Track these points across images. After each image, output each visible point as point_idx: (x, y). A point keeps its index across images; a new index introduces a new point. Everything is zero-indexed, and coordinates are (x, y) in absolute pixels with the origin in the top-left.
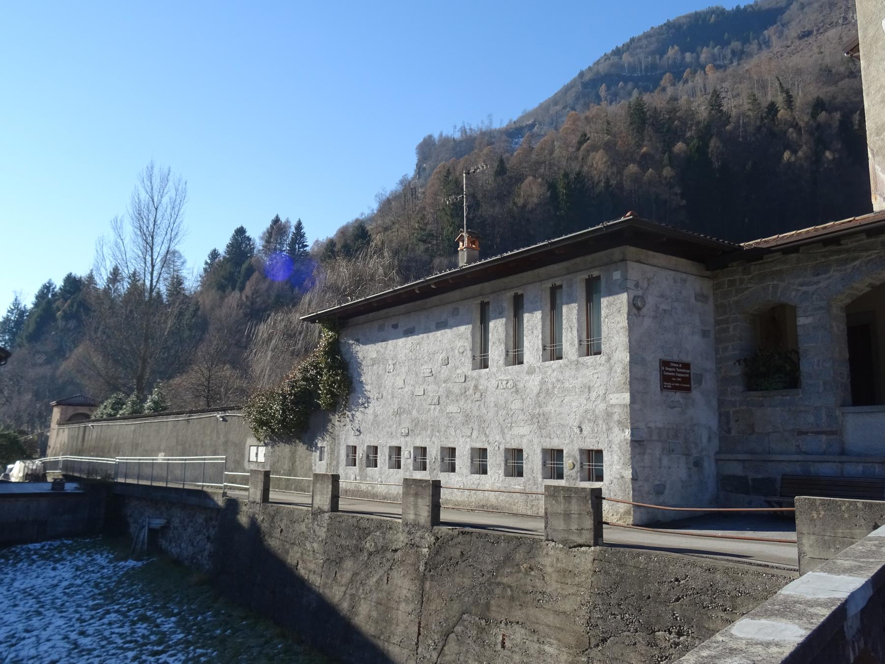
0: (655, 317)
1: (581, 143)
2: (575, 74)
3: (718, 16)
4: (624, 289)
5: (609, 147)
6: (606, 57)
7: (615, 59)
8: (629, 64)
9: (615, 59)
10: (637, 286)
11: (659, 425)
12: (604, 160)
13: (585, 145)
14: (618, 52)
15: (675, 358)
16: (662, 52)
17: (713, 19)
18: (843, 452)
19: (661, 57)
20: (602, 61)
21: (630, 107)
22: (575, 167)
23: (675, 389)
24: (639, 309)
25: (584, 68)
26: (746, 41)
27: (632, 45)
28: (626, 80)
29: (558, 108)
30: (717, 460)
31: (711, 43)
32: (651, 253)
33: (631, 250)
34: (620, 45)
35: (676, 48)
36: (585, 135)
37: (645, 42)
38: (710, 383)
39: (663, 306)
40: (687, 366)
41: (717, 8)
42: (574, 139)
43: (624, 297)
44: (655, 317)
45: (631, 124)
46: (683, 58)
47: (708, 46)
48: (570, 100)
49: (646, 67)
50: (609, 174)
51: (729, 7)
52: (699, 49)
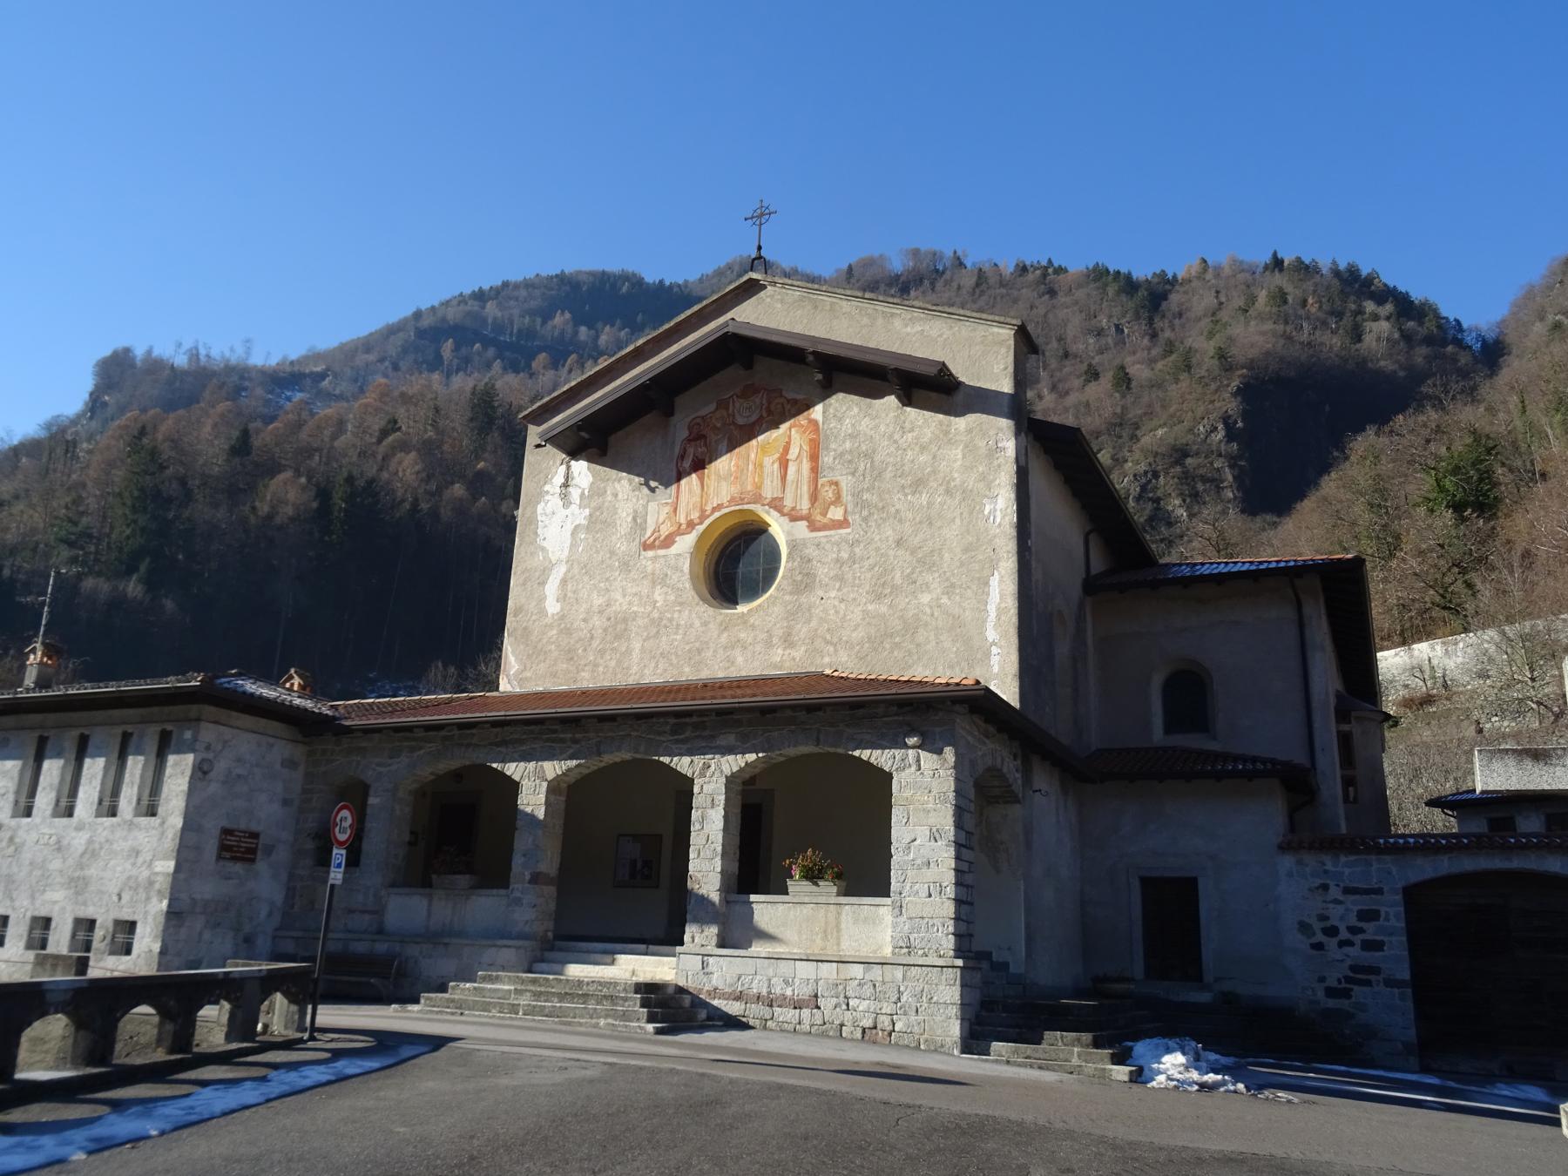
0: (224, 783)
2: (408, 312)
3: (633, 285)
4: (193, 750)
10: (208, 748)
11: (207, 896)
15: (243, 826)
17: (624, 289)
18: (381, 931)
23: (233, 859)
24: (205, 773)
30: (274, 938)
32: (234, 714)
33: (209, 710)
36: (396, 422)
38: (282, 855)
39: (239, 771)
40: (255, 835)
43: (190, 758)
44: (224, 783)
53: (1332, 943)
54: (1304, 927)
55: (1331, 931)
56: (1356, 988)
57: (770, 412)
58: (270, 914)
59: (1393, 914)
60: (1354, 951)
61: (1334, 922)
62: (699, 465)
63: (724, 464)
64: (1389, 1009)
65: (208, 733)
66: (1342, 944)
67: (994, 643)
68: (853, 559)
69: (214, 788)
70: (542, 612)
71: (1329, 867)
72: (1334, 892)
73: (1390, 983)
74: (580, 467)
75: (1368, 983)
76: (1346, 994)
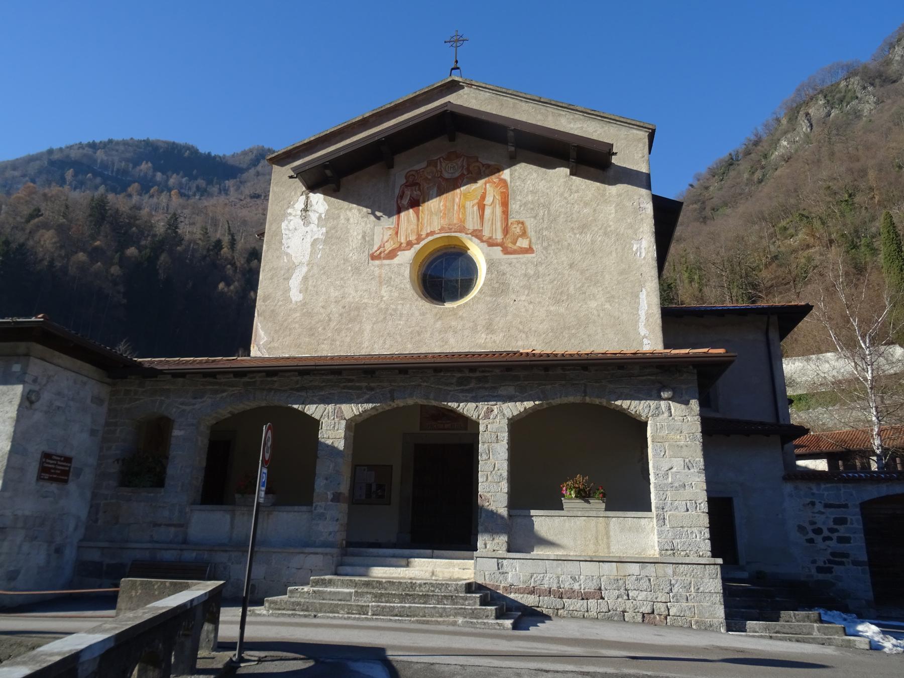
0: (46, 412)
1: (32, 217)
4: (20, 380)
5: (61, 230)
6: (81, 146)
7: (89, 151)
8: (102, 161)
9: (89, 151)
10: (35, 381)
11: (27, 513)
12: (54, 240)
13: (36, 220)
14: (93, 146)
15: (59, 452)
16: (136, 163)
18: (185, 542)
19: (134, 167)
20: (76, 147)
21: (92, 200)
22: (20, 237)
23: (51, 480)
24: (32, 403)
25: (56, 146)
26: (210, 182)
27: (108, 145)
28: (96, 174)
29: (16, 173)
30: (79, 547)
31: (181, 173)
32: (57, 353)
33: (38, 348)
34: (97, 141)
35: (150, 164)
37: (122, 148)
38: (88, 476)
39: (58, 403)
40: (68, 460)
41: (193, 147)
42: (26, 211)
43: (19, 389)
44: (46, 412)
45: (90, 215)
46: (154, 176)
47: (178, 174)
48: (32, 169)
49: (118, 170)
50: (56, 255)
51: (203, 149)
52: (169, 173)
53: (818, 539)
54: (801, 529)
55: (818, 531)
56: (835, 566)
57: (469, 171)
58: (76, 528)
59: (855, 520)
60: (833, 544)
61: (819, 525)
62: (415, 203)
63: (434, 205)
64: (856, 579)
65: (36, 367)
66: (826, 539)
67: (645, 337)
68: (537, 275)
69: (38, 416)
70: (288, 300)
71: (815, 491)
72: (819, 507)
73: (856, 563)
74: (318, 200)
75: (842, 563)
76: (829, 570)
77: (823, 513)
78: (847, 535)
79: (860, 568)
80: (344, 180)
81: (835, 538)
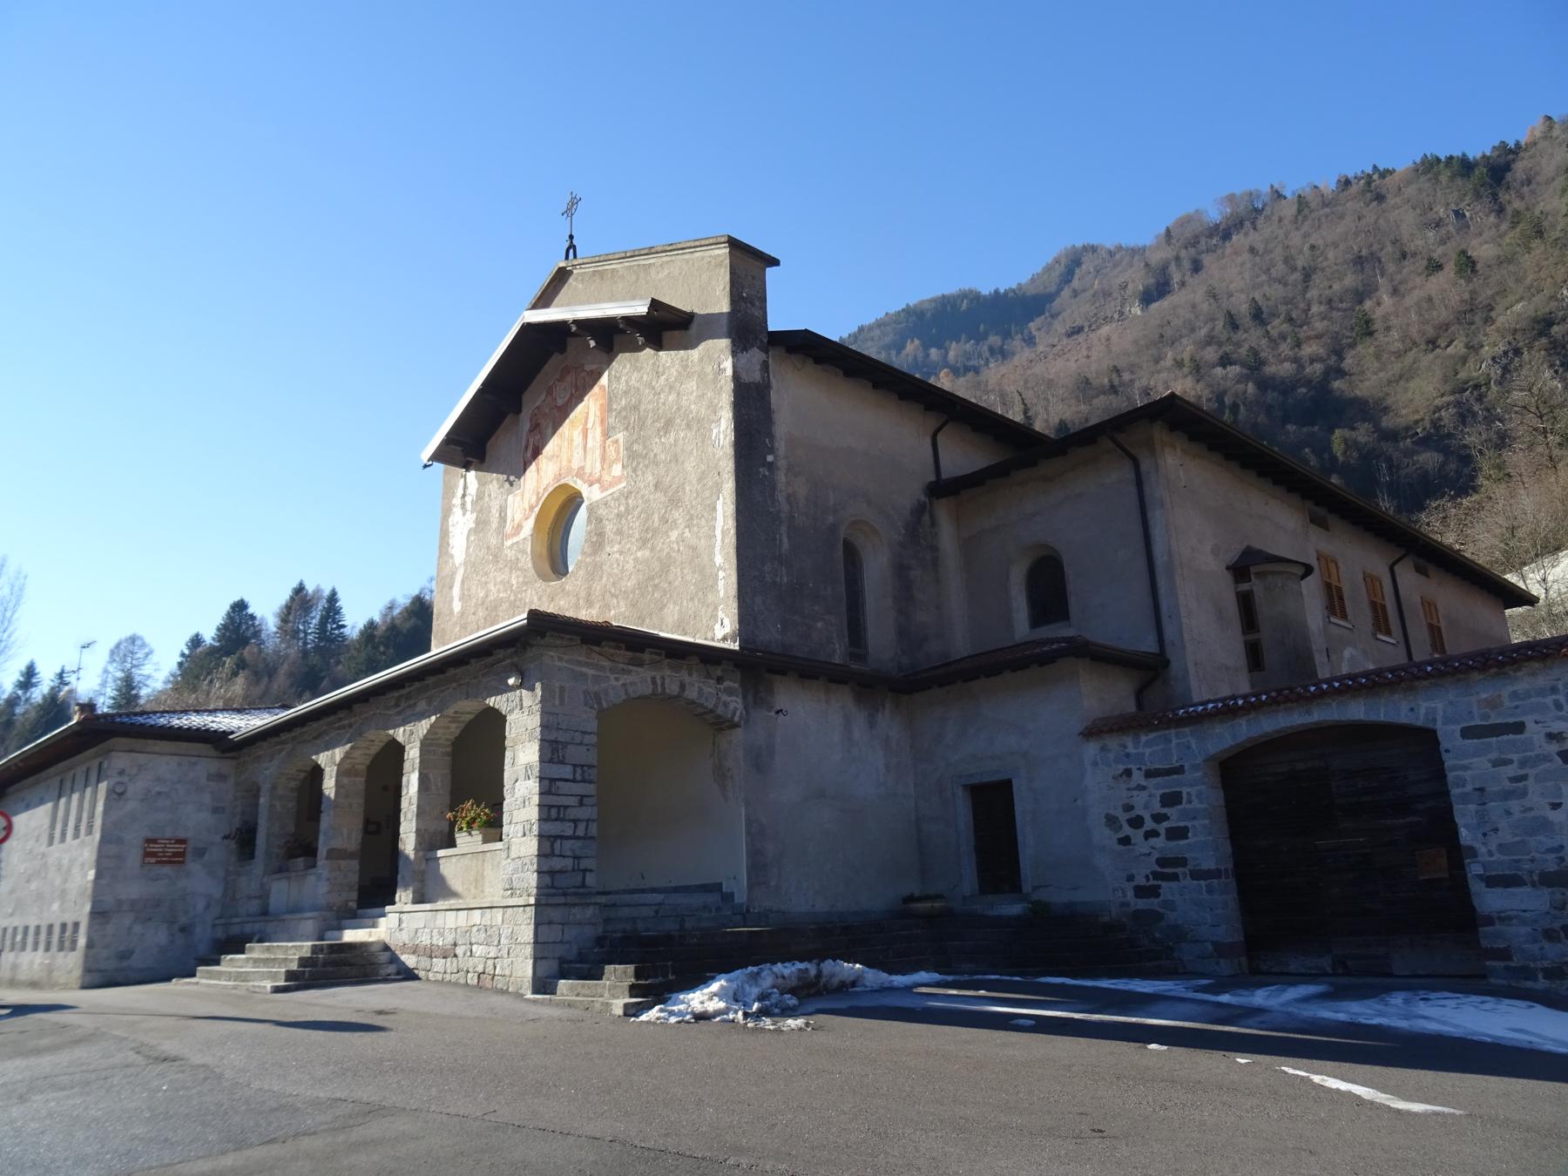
15: (167, 835)
39: (158, 789)
40: (183, 841)
53: (1137, 835)
54: (1111, 821)
55: (1136, 822)
56: (1163, 884)
57: (577, 388)
58: (208, 906)
59: (1202, 798)
60: (1159, 842)
61: (1139, 811)
62: (537, 452)
63: (550, 448)
65: (120, 760)
66: (1150, 834)
67: (720, 568)
68: (628, 511)
69: (131, 805)
71: (1131, 750)
72: (1138, 777)
73: (1197, 875)
75: (1175, 877)
76: (1153, 892)
77: (1144, 788)
78: (1182, 824)
79: (1203, 883)
80: (488, 445)
81: (1163, 832)
